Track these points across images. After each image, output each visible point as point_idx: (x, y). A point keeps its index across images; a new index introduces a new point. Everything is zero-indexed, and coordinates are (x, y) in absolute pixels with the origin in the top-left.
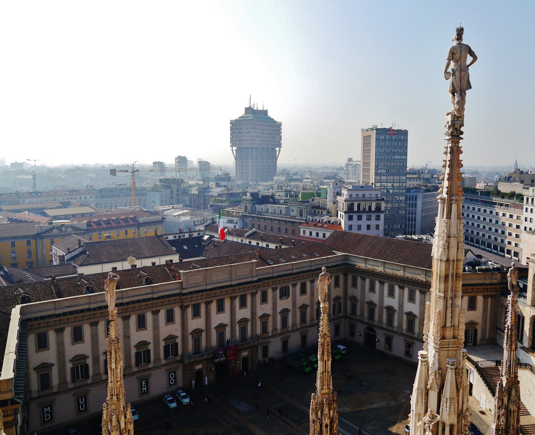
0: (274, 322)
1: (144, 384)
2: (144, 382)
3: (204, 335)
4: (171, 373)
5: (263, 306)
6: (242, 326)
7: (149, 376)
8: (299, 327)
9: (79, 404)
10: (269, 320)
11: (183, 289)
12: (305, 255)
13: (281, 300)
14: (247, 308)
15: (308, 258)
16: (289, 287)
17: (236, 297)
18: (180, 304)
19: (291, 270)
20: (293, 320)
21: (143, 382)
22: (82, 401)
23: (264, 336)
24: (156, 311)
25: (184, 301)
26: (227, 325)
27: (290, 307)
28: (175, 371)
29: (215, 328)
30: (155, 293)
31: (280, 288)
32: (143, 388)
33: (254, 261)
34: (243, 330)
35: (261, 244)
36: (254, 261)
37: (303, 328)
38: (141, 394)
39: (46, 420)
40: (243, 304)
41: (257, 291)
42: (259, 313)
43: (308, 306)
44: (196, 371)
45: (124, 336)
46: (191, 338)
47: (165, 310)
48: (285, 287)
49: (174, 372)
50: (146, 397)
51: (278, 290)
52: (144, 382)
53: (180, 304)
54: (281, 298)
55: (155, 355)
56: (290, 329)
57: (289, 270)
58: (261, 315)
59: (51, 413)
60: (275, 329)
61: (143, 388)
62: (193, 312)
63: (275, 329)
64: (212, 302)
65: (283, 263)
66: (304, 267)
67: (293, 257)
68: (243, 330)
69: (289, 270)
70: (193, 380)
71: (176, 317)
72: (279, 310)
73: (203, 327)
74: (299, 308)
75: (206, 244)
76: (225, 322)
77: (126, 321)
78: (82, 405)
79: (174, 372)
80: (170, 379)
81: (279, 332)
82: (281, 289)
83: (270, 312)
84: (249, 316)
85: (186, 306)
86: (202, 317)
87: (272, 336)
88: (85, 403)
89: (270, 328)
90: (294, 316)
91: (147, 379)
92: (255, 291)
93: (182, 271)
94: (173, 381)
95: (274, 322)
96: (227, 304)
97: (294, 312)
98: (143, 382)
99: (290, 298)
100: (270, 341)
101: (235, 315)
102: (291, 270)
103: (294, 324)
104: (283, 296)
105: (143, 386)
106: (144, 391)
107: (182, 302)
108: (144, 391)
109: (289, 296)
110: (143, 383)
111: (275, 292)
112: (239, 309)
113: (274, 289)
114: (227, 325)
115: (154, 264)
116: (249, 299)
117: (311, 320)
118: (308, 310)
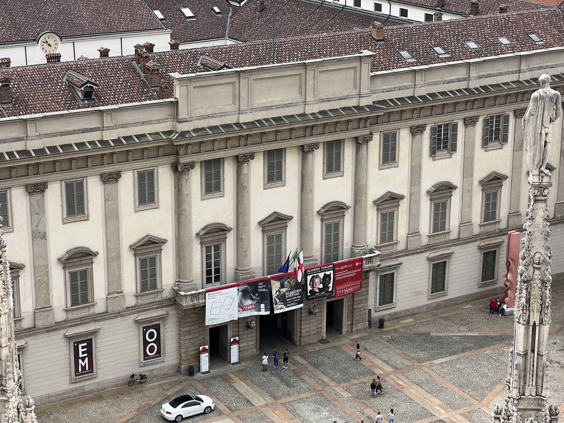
0: (414, 216)
1: (83, 353)
2: (83, 348)
3: (231, 239)
4: (148, 328)
7: (95, 333)
8: (477, 230)
11: (180, 122)
12: (504, 41)
13: (434, 160)
14: (343, 176)
15: (513, 49)
16: (455, 127)
17: (316, 146)
18: (171, 159)
19: (464, 80)
21: (80, 346)
24: (110, 174)
25: (182, 151)
26: (290, 218)
27: (456, 180)
29: (131, 247)
30: (109, 128)
31: (433, 130)
32: (80, 360)
33: (366, 53)
35: (385, 10)
36: (366, 53)
37: (489, 235)
38: (76, 376)
41: (371, 134)
43: (505, 178)
45: (33, 232)
46: (199, 246)
47: (134, 173)
48: (446, 125)
49: (157, 327)
50: (88, 385)
51: (427, 134)
52: (83, 348)
53: (171, 159)
54: (433, 153)
56: (454, 235)
57: (459, 80)
60: (414, 233)
61: (80, 360)
62: (204, 180)
63: (414, 233)
64: (252, 156)
65: (443, 60)
67: (472, 45)
69: (459, 80)
70: (204, 350)
71: (160, 193)
72: (427, 184)
73: (229, 220)
74: (481, 182)
75: (242, 4)
76: (285, 211)
77: (37, 197)
80: (146, 343)
81: (425, 241)
82: (436, 131)
83: (402, 189)
84: (348, 199)
85: (185, 165)
86: (226, 195)
87: (407, 252)
90: (466, 204)
91: (91, 339)
92: (367, 132)
93: (176, 75)
94: (153, 346)
97: (468, 191)
99: (458, 155)
100: (401, 264)
102: (464, 80)
103: (465, 223)
104: (439, 148)
105: (81, 355)
106: (84, 368)
107: (177, 154)
108: (84, 368)
109: (454, 149)
110: (81, 350)
111: (418, 137)
112: (322, 178)
113: (416, 131)
114: (290, 218)
115: (104, 53)
116: (348, 152)
117: (510, 215)
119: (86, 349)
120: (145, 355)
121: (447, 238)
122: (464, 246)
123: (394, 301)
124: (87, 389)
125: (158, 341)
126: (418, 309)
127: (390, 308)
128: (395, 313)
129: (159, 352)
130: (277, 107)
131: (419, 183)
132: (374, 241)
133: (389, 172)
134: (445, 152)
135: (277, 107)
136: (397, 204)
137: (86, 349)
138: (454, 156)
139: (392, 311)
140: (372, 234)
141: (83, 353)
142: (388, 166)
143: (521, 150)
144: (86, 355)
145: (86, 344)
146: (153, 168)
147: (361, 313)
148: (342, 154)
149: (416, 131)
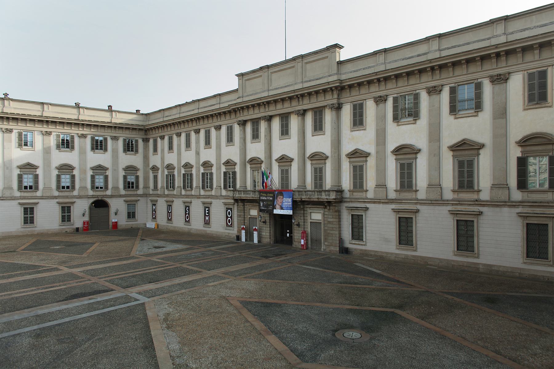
0: (381, 171)
1: (207, 213)
2: (207, 210)
5: (356, 134)
6: (317, 166)
9: (168, 212)
10: (368, 163)
13: (398, 125)
20: (430, 177)
21: (207, 209)
22: (170, 211)
23: (357, 195)
28: (232, 209)
34: (319, 175)
39: (154, 217)
40: (318, 127)
42: (347, 147)
44: (250, 216)
50: (208, 230)
51: (390, 102)
52: (207, 210)
54: (396, 118)
55: (217, 181)
58: (350, 151)
59: (155, 212)
60: (381, 185)
63: (381, 185)
66: (468, 44)
68: (319, 175)
72: (391, 146)
76: (291, 155)
77: (197, 135)
78: (170, 213)
79: (231, 209)
80: (227, 217)
88: (171, 212)
89: (370, 181)
94: (229, 220)
95: (381, 171)
96: (294, 122)
98: (207, 209)
101: (299, 141)
105: (207, 214)
106: (207, 221)
110: (207, 212)
111: (381, 105)
113: (380, 100)
118: (481, 157)
119: (208, 212)
120: (227, 224)
121: (414, 197)
122: (432, 207)
123: (364, 240)
124: (208, 232)
125: (231, 217)
126: (387, 254)
127: (362, 245)
128: (366, 250)
129: (231, 224)
130: (281, 88)
131: (384, 143)
132: (348, 186)
133: (358, 134)
134: (411, 119)
135: (281, 88)
136: (364, 159)
137: (208, 212)
138: (418, 122)
139: (363, 248)
140: (346, 180)
141: (207, 213)
142: (358, 129)
143: (503, 118)
144: (208, 214)
145: (208, 209)
146: (232, 124)
147: (333, 238)
148: (323, 119)
149: (380, 100)
